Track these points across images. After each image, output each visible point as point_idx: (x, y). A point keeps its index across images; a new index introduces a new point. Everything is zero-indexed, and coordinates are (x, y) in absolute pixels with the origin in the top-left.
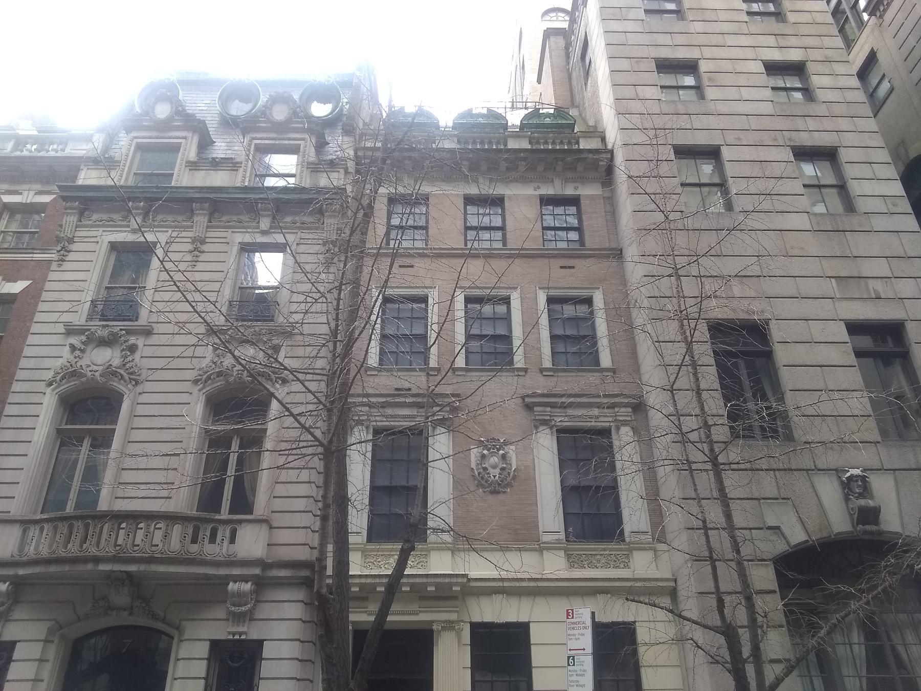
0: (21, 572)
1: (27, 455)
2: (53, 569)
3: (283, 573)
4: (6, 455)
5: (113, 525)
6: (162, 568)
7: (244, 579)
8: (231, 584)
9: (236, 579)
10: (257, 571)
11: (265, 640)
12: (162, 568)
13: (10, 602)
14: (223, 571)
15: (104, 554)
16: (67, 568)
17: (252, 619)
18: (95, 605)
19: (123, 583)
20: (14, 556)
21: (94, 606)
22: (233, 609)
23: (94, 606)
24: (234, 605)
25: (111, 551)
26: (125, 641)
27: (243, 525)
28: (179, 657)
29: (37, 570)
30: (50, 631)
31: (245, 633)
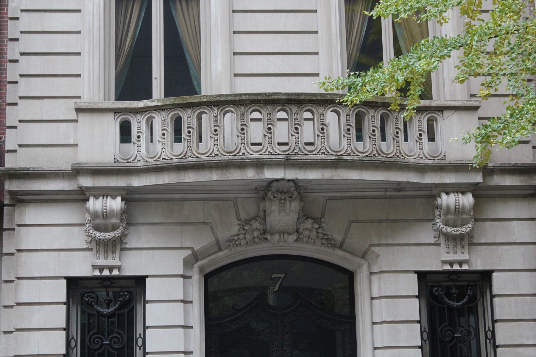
0: (137, 182)
1: (79, 11)
2: (191, 177)
3: (509, 181)
4: (45, 11)
5: (270, 114)
6: (354, 175)
7: (461, 189)
8: (444, 196)
9: (448, 189)
10: (478, 178)
11: (493, 271)
12: (354, 175)
13: (124, 225)
14: (430, 179)
15: (268, 157)
16: (214, 176)
17: (471, 244)
18: (247, 227)
19: (291, 197)
20: (118, 161)
21: (244, 229)
22: (449, 230)
23: (244, 229)
24: (447, 224)
25: (280, 153)
26: (274, 276)
27: (446, 113)
28: (374, 296)
29: (165, 179)
30: (188, 263)
31: (466, 262)
